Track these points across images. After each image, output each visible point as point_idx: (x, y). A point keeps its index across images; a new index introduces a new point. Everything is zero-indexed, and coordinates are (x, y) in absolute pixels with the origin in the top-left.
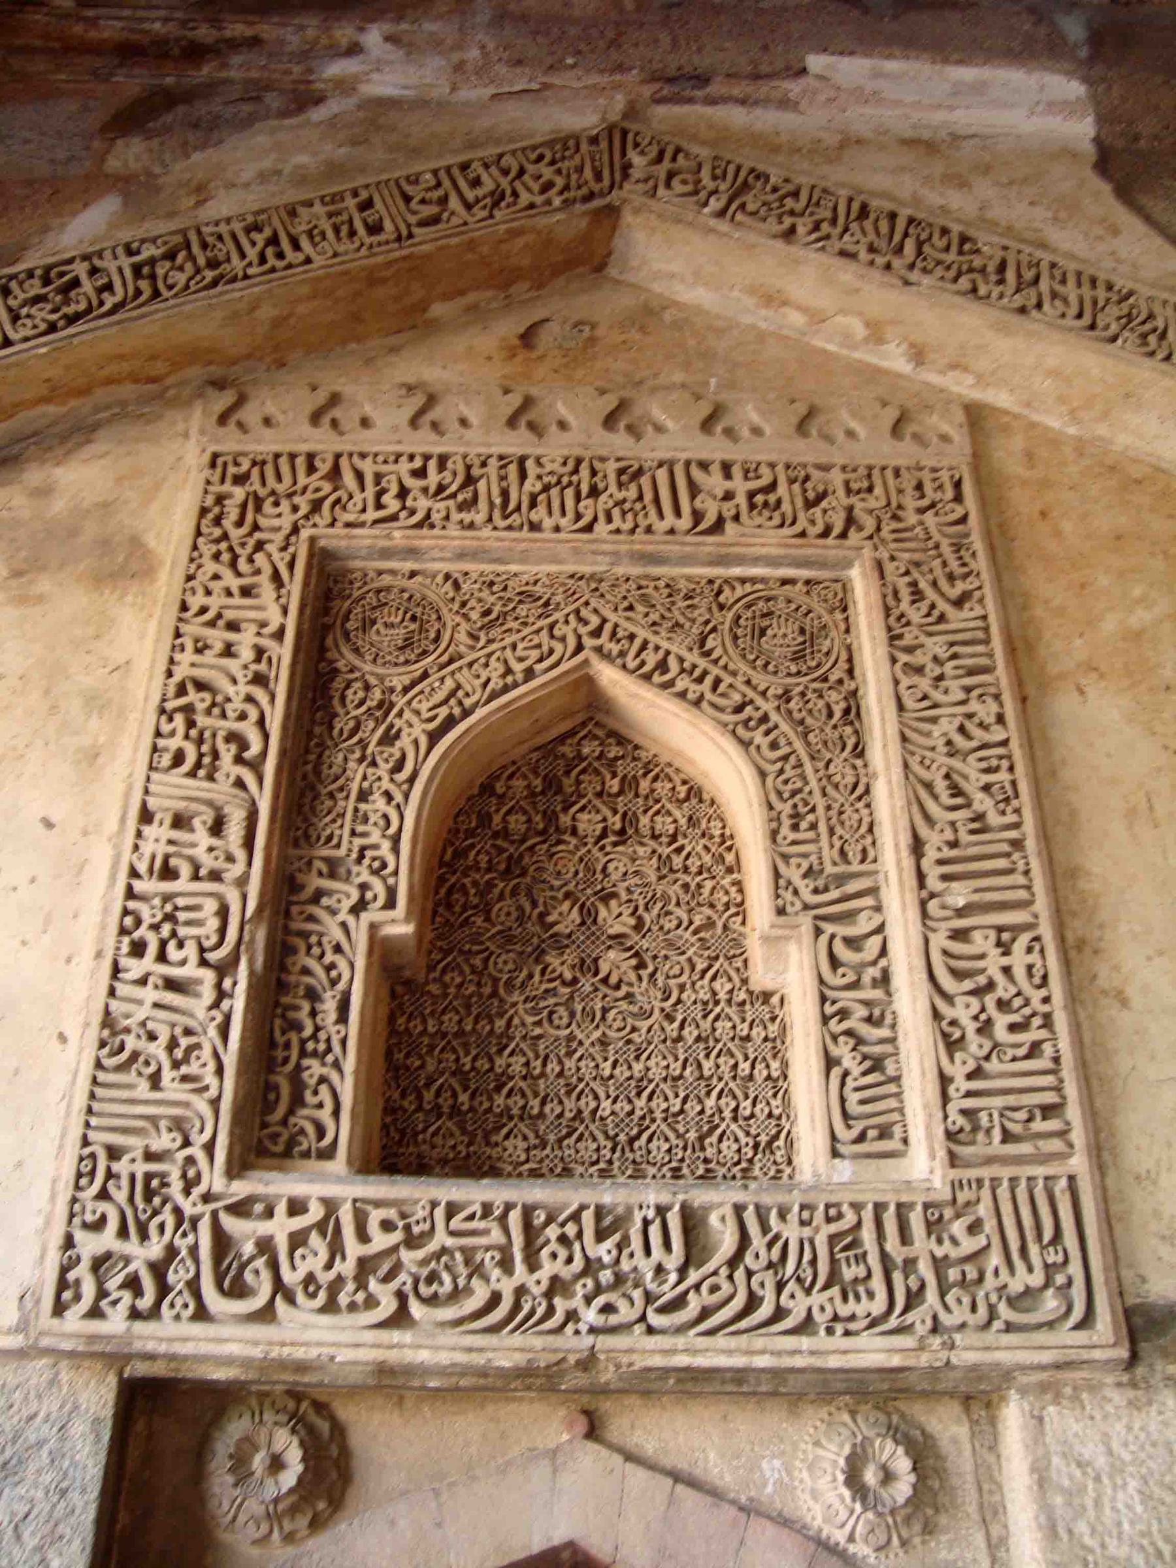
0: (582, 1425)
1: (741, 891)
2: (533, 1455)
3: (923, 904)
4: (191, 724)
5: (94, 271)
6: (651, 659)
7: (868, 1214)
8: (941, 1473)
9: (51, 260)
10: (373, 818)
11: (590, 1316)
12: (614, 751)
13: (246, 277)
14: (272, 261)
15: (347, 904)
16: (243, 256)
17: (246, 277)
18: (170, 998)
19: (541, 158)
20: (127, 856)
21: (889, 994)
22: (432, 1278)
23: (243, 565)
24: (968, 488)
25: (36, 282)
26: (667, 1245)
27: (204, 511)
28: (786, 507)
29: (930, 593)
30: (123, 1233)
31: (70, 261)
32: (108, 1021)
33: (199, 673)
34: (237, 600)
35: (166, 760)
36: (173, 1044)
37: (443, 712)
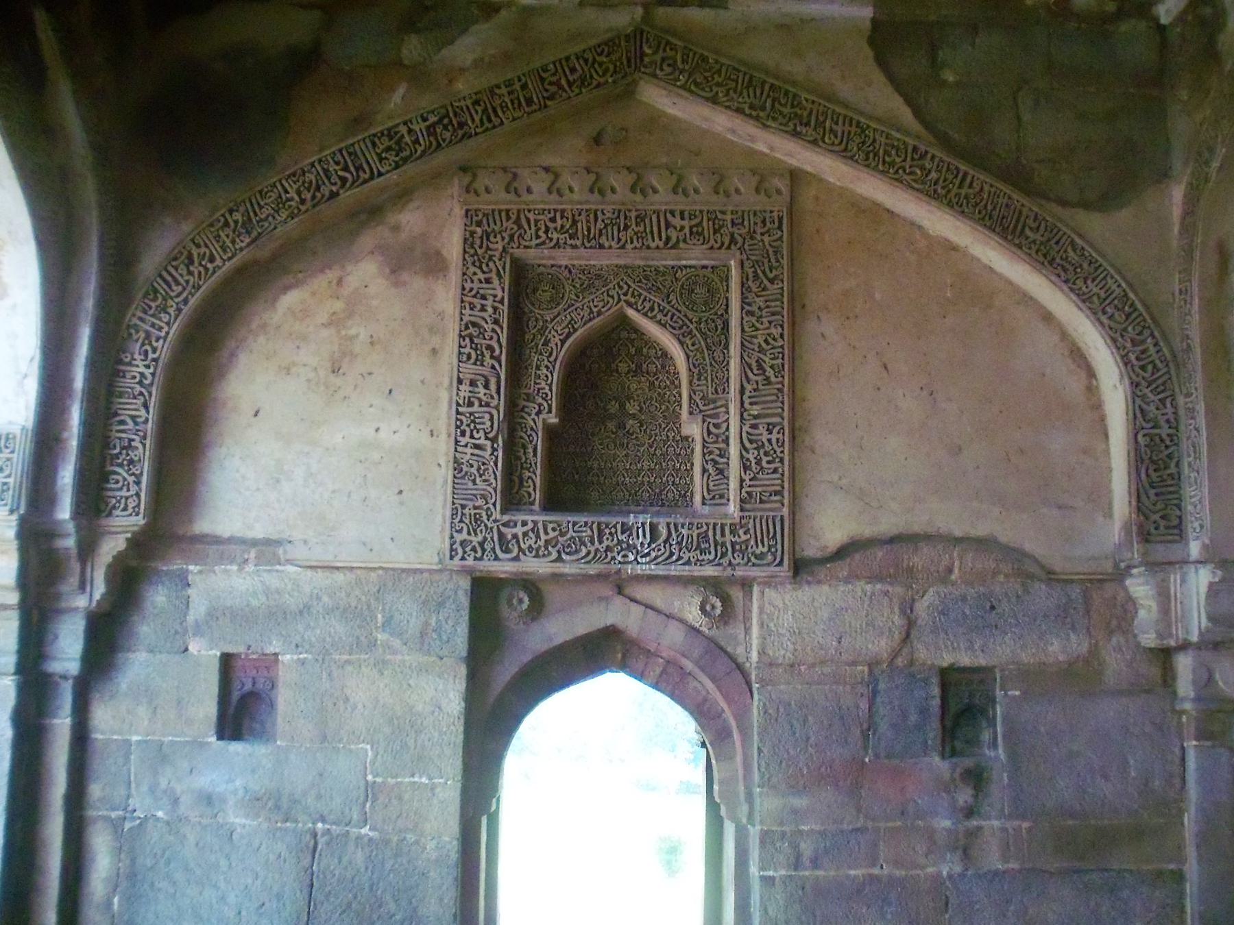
0: (616, 590)
1: (680, 396)
2: (601, 599)
3: (742, 415)
4: (472, 341)
5: (410, 131)
6: (648, 305)
7: (711, 527)
8: (732, 607)
9: (390, 124)
10: (543, 377)
11: (619, 558)
12: (634, 336)
13: (476, 134)
14: (487, 125)
15: (534, 411)
16: (473, 120)
17: (476, 134)
18: (476, 452)
19: (603, 51)
20: (455, 398)
21: (728, 445)
22: (569, 546)
23: (484, 266)
24: (785, 221)
25: (386, 139)
26: (644, 536)
27: (465, 240)
28: (706, 232)
29: (761, 275)
30: (469, 533)
31: (398, 125)
32: (456, 461)
33: (473, 319)
34: (484, 285)
35: (465, 358)
36: (478, 470)
37: (567, 330)
